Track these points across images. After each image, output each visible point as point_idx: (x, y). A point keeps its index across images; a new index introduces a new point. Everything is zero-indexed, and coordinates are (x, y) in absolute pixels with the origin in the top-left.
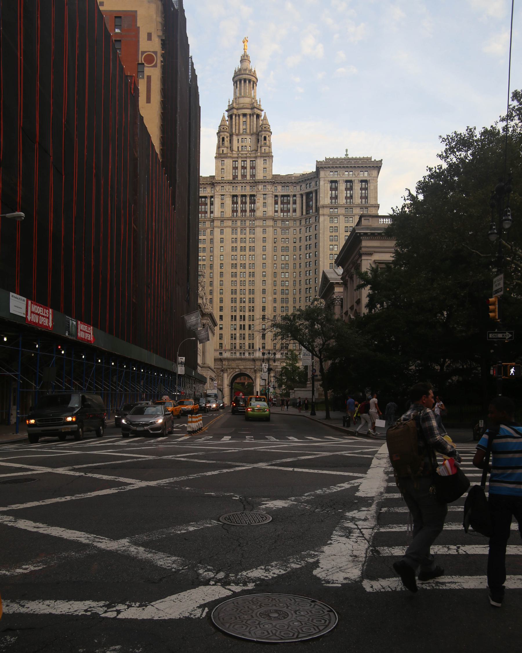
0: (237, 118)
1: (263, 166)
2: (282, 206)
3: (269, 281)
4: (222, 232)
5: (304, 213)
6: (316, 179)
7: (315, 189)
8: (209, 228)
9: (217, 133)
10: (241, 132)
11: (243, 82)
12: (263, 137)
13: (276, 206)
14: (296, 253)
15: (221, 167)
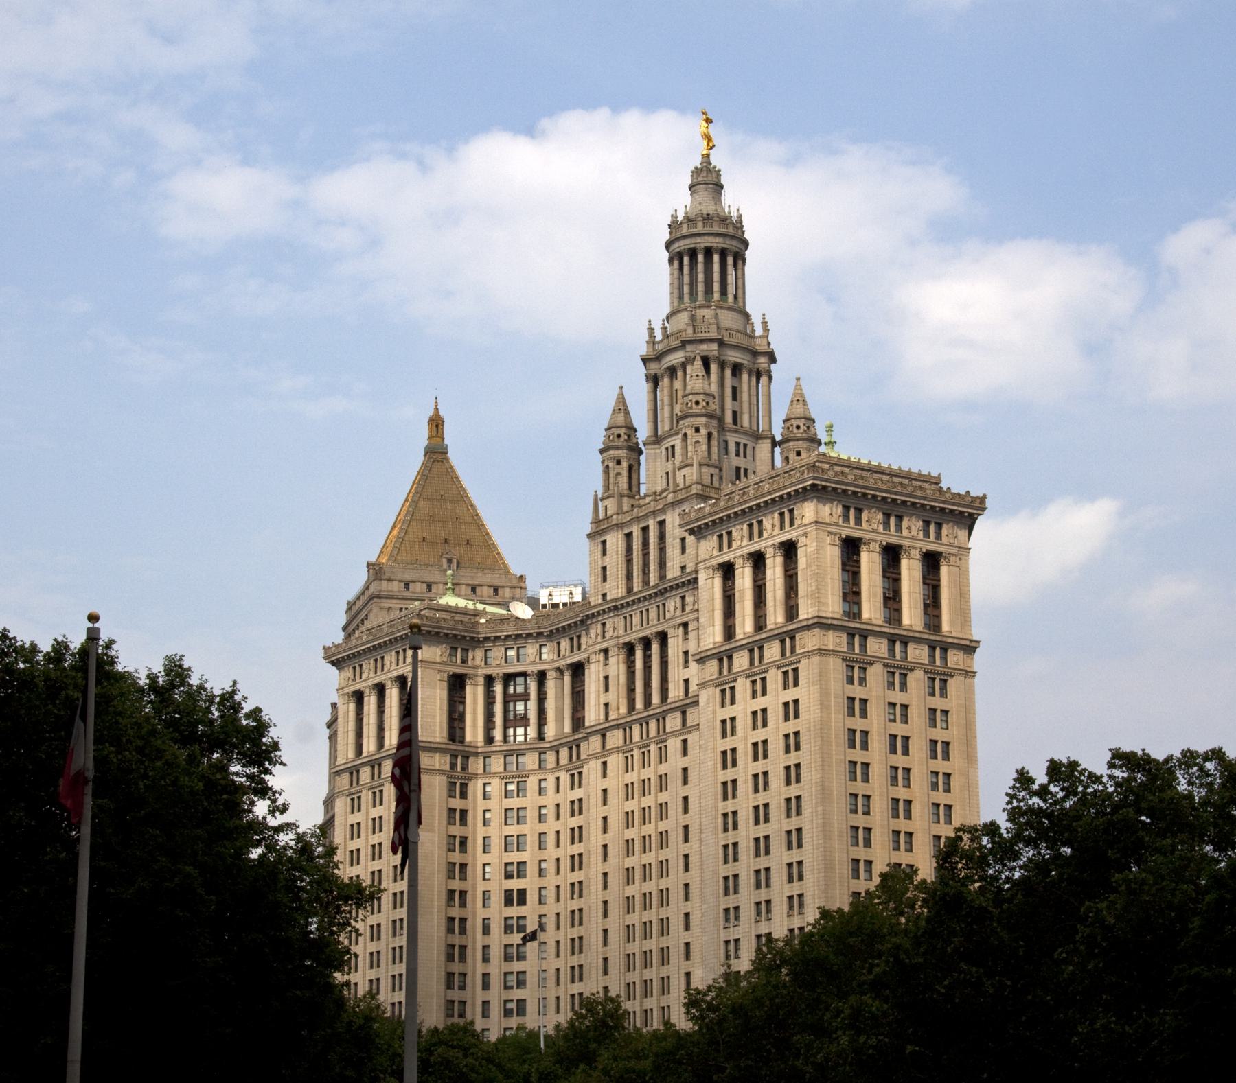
15: (600, 565)
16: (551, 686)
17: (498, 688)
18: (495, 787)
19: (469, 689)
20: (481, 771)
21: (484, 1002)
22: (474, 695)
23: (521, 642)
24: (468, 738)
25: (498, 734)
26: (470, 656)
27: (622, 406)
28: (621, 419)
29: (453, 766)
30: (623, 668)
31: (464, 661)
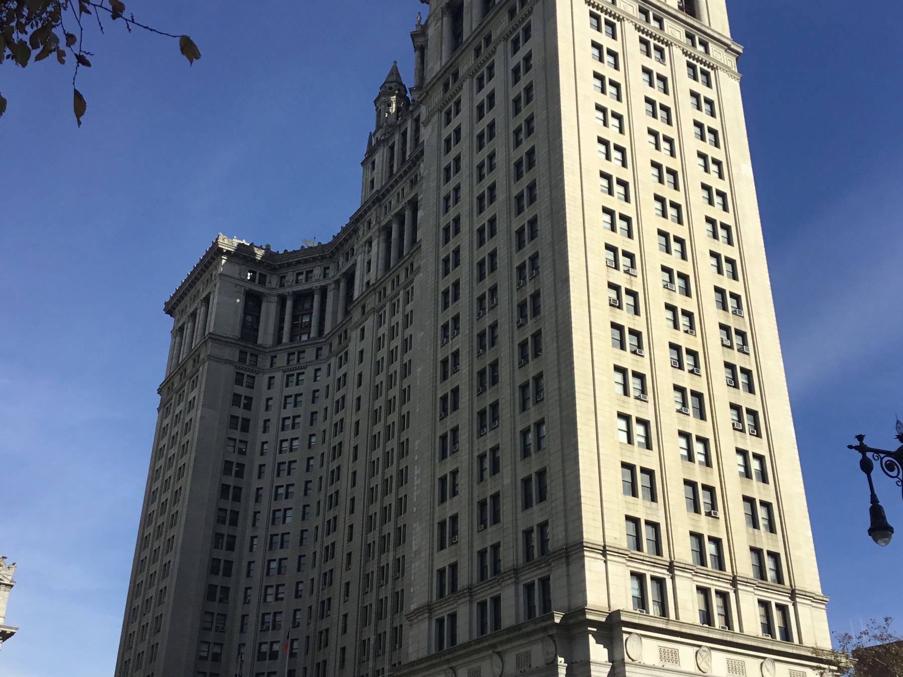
15: (370, 179)
16: (330, 295)
17: (289, 304)
18: (279, 377)
19: (264, 305)
20: (268, 366)
21: (250, 563)
22: (269, 310)
23: (308, 267)
24: (259, 342)
25: (285, 339)
26: (268, 280)
27: (395, 72)
28: (394, 78)
29: (242, 359)
30: (382, 246)
31: (262, 282)
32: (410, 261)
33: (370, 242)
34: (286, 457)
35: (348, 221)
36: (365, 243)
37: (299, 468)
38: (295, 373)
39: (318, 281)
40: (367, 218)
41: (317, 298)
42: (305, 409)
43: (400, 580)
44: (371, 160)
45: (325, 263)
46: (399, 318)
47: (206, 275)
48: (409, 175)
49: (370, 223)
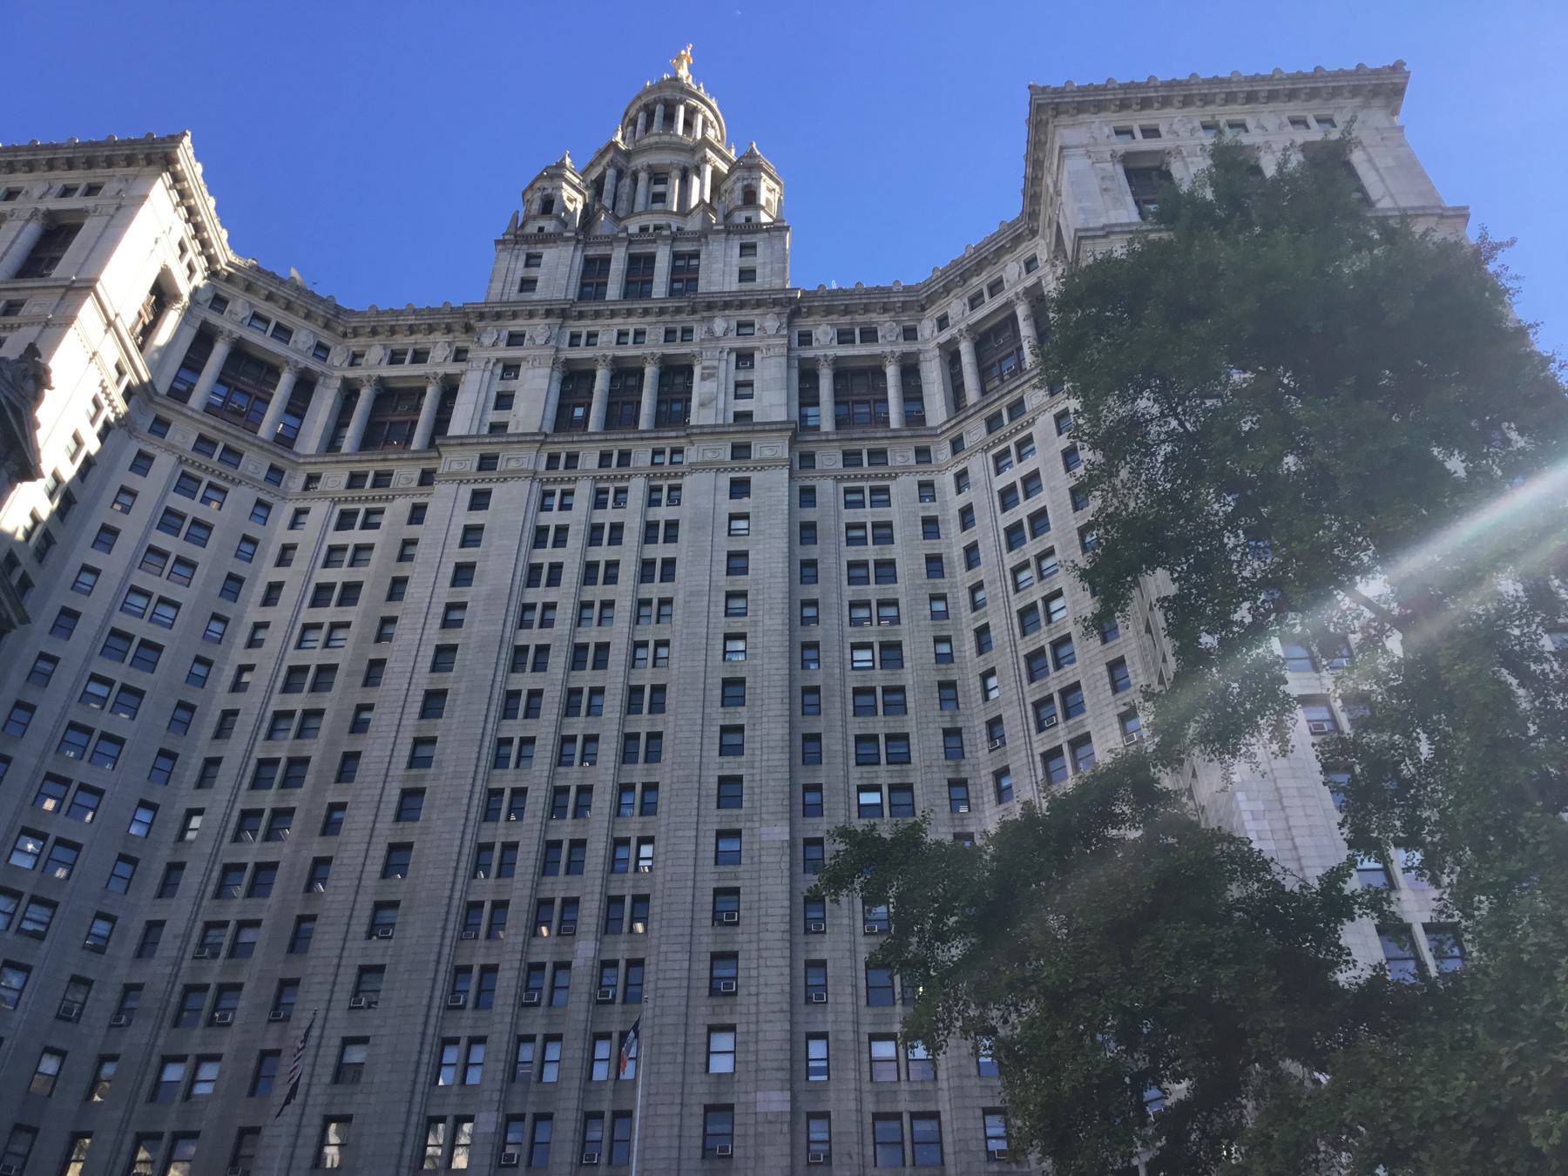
0: (627, 181)
1: (735, 261)
2: (843, 410)
3: (768, 723)
4: (480, 500)
5: (972, 394)
6: (1025, 251)
7: (1030, 281)
8: (405, 493)
9: (524, 194)
10: (639, 206)
11: (659, 110)
12: (740, 185)
13: (811, 411)
14: (942, 585)
15: (520, 271)
17: (220, 351)
18: (164, 465)
32: (676, 443)
33: (511, 369)
34: (140, 629)
35: (437, 304)
36: (498, 360)
37: (174, 665)
38: (206, 479)
39: (299, 352)
40: (516, 326)
41: (286, 381)
42: (212, 559)
43: (618, 1007)
44: (523, 250)
45: (326, 338)
46: (632, 516)
47: (79, 178)
48: (667, 318)
49: (515, 339)
